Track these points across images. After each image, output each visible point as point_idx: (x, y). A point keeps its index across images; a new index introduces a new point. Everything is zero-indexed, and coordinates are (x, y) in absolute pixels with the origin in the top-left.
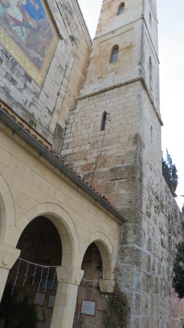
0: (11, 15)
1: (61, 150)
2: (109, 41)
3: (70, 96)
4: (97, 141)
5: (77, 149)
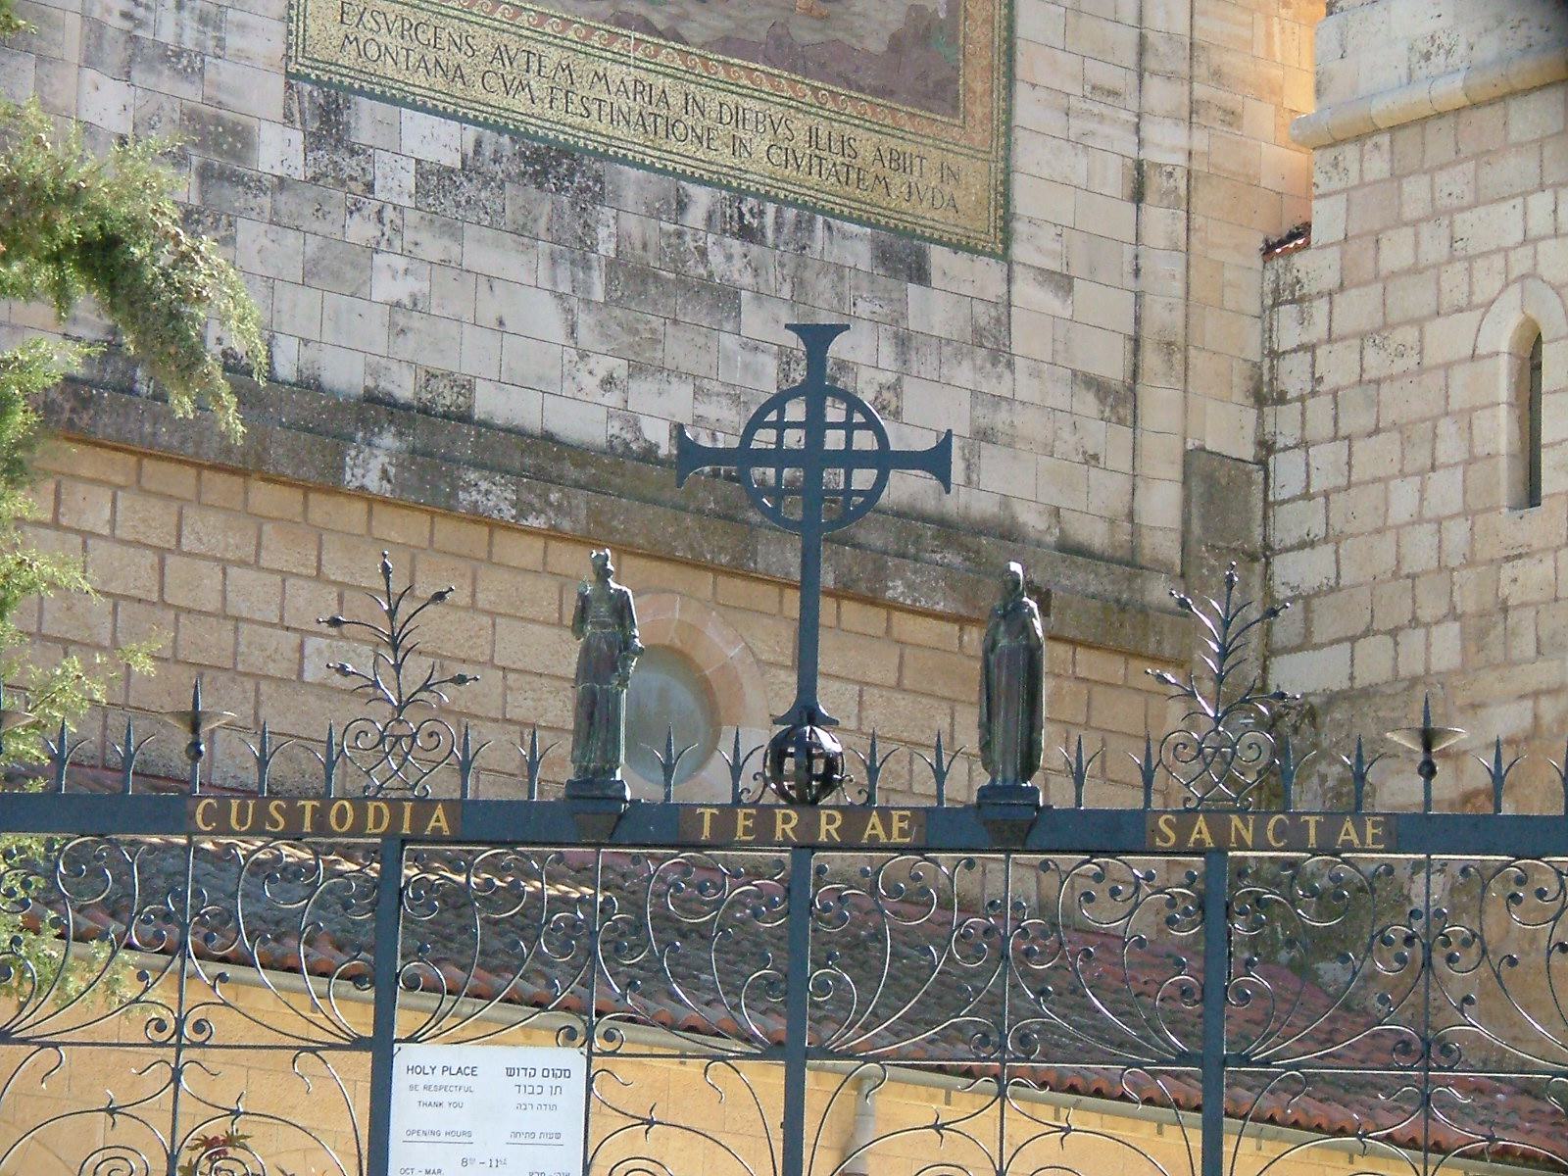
1: (1269, 652)
4: (1505, 609)
5: (1374, 662)
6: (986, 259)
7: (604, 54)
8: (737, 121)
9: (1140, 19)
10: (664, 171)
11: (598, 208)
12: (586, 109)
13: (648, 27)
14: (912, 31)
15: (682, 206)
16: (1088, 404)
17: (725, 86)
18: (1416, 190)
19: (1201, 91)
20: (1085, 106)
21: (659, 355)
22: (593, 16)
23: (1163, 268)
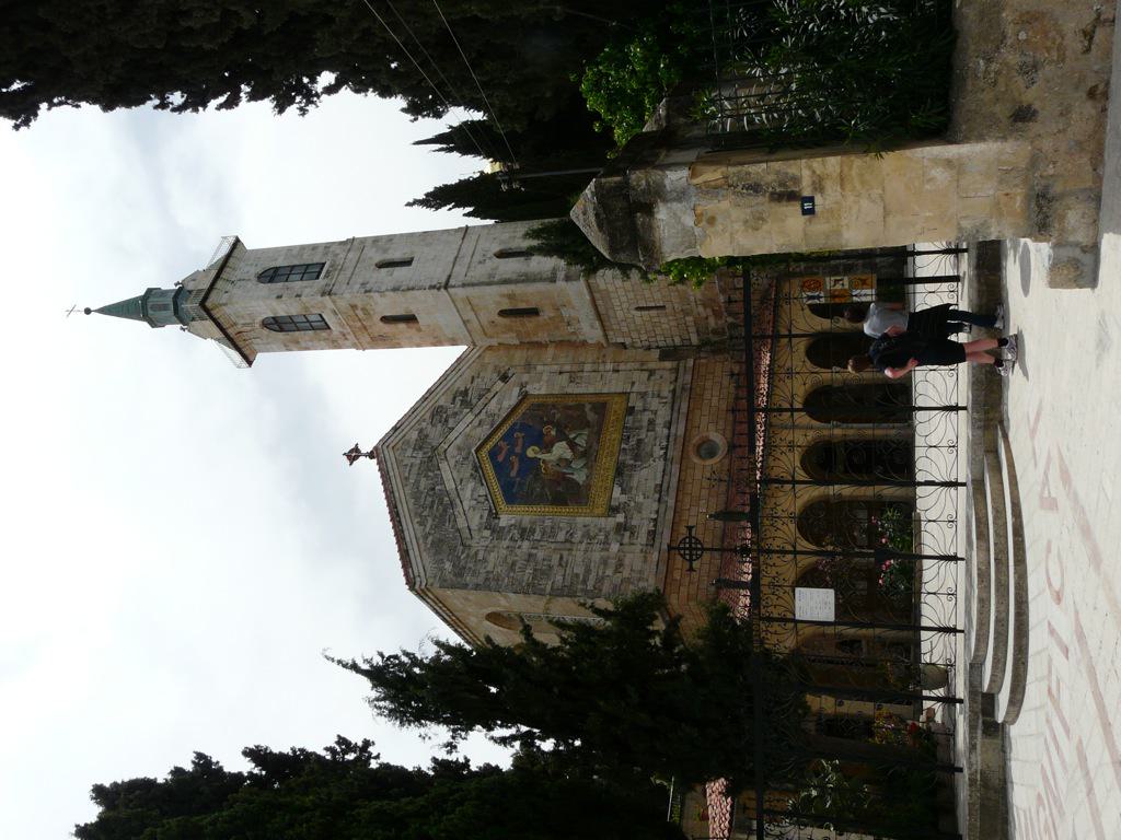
1: (691, 345)
2: (485, 323)
3: (604, 356)
5: (692, 329)
15: (624, 449)
16: (653, 378)
18: (614, 327)
23: (629, 366)
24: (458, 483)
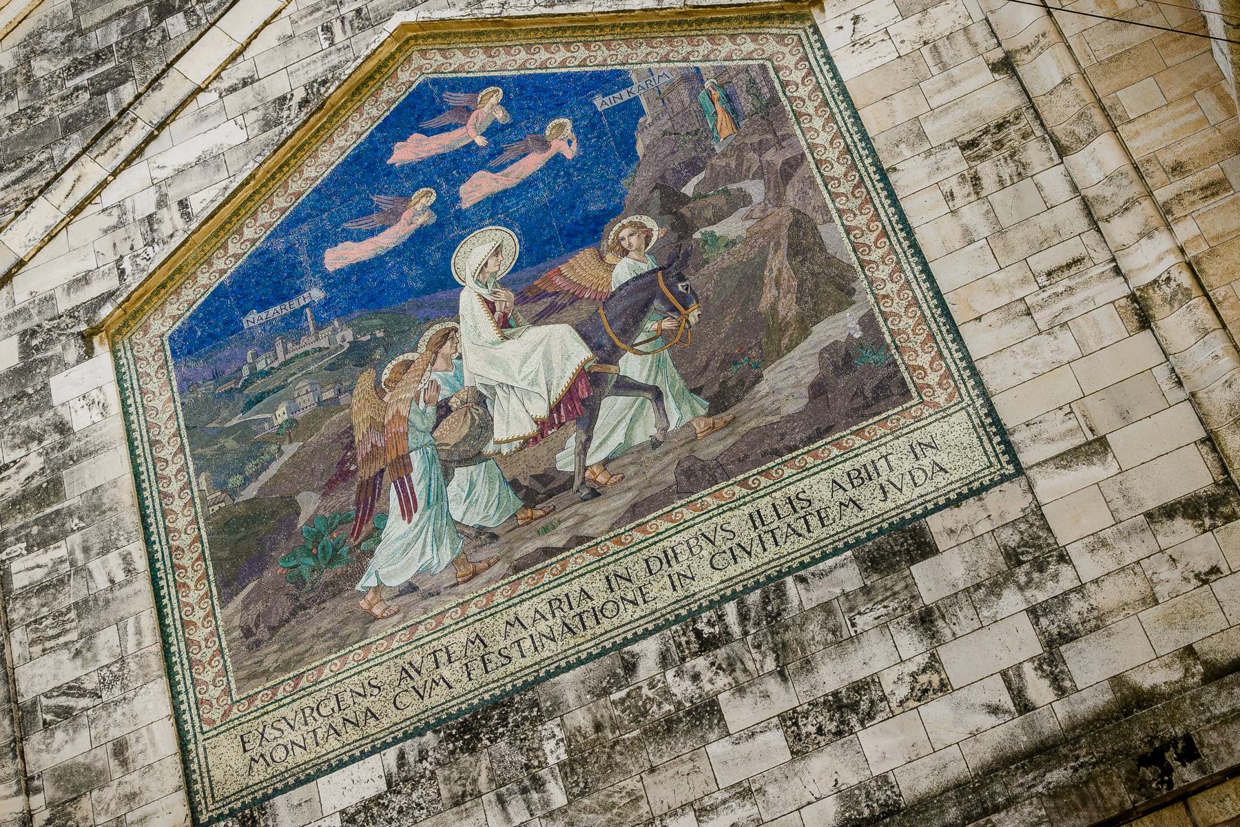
0: (530, 429)
3: (1214, 188)
6: (998, 488)
7: (510, 603)
8: (668, 562)
9: (1075, 188)
10: (604, 652)
11: (540, 728)
12: (505, 657)
13: (549, 552)
14: (831, 368)
15: (630, 667)
16: (1182, 527)
17: (646, 544)
19: (1162, 195)
20: (1045, 295)
21: (646, 808)
22: (489, 582)
24: (229, 78)
